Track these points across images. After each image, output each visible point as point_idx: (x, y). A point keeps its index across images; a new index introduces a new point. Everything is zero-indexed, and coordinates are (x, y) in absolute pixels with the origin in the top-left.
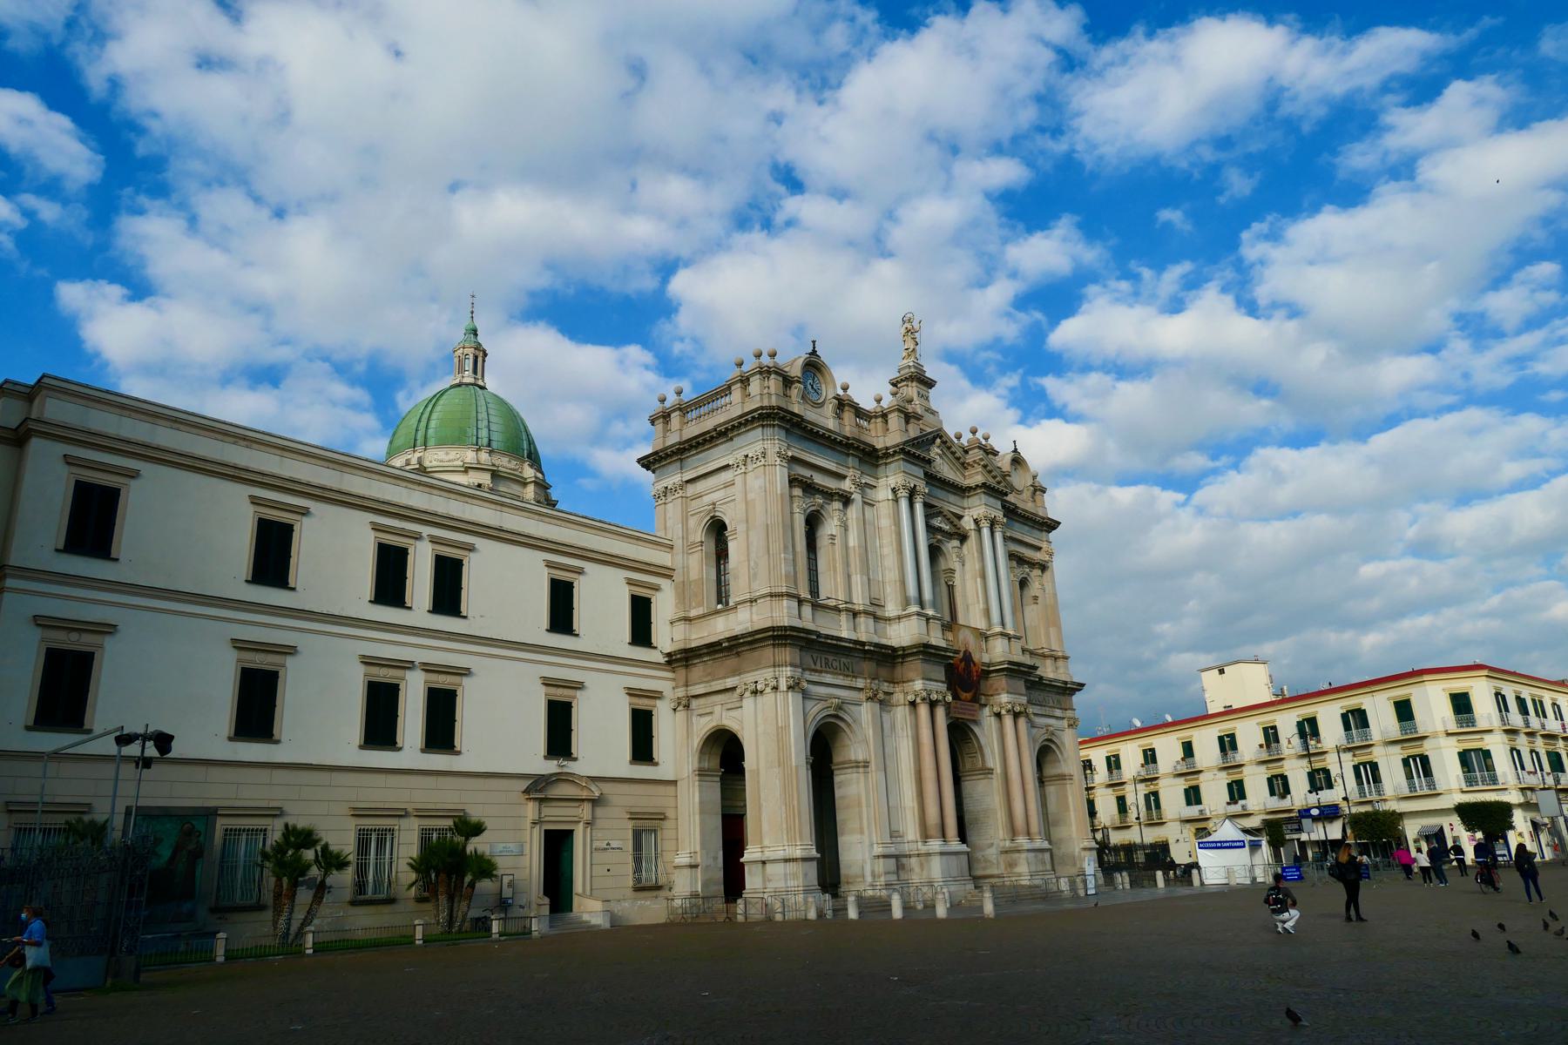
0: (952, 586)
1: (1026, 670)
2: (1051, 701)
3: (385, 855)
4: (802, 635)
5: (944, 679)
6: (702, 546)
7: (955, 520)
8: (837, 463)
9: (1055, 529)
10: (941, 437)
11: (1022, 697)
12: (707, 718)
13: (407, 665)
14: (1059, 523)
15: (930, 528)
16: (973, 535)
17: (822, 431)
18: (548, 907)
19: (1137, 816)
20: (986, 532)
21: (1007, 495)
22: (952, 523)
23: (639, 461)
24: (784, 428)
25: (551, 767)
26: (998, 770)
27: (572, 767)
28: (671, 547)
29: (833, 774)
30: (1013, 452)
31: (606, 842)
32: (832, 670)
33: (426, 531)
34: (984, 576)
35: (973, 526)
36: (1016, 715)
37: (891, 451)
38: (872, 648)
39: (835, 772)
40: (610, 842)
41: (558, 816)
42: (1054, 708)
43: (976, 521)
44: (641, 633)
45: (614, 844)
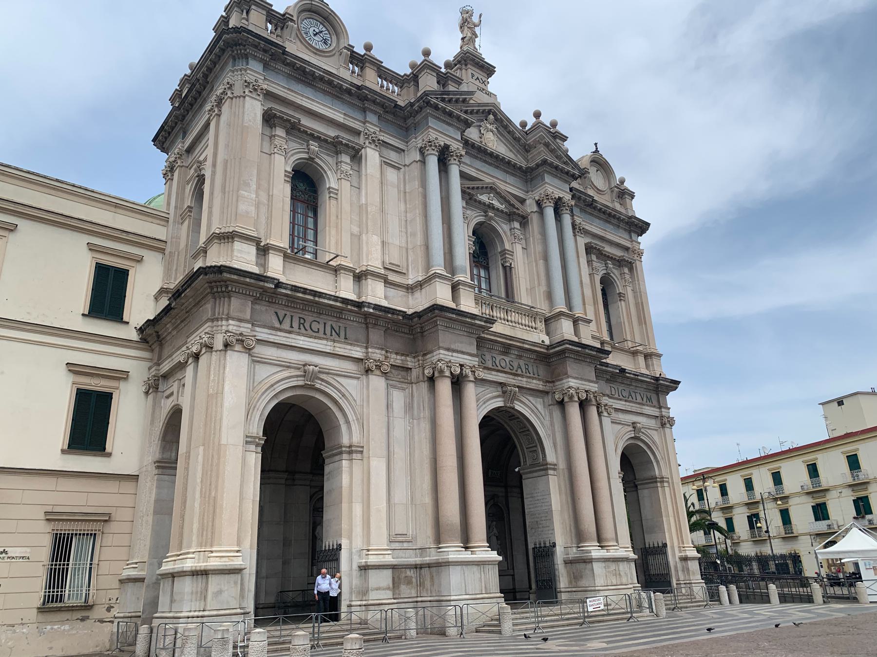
0: (511, 268)
2: (639, 398)
4: (248, 280)
5: (475, 352)
6: (191, 212)
7: (517, 204)
8: (345, 114)
10: (495, 115)
11: (591, 384)
16: (535, 219)
19: (766, 529)
20: (550, 212)
26: (562, 465)
28: (167, 220)
29: (324, 460)
32: (310, 332)
34: (546, 258)
35: (535, 209)
36: (583, 405)
37: (416, 107)
38: (371, 310)
39: (326, 461)
40: (7, 549)
42: (643, 405)
43: (539, 204)
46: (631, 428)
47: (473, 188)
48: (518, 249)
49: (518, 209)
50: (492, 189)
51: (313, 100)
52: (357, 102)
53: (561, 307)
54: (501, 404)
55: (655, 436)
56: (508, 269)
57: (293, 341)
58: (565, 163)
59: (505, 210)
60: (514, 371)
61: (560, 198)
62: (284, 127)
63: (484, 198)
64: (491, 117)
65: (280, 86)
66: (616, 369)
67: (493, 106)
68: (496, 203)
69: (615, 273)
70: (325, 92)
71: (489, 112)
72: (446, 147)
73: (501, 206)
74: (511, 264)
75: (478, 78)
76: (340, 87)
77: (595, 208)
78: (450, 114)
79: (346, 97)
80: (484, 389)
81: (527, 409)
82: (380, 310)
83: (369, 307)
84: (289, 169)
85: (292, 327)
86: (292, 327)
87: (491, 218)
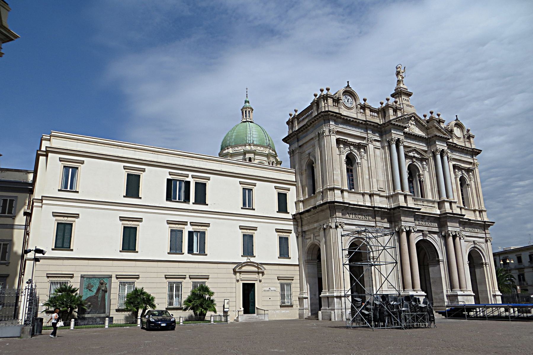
3: (173, 292)
7: (423, 153)
9: (479, 153)
10: (414, 117)
12: (309, 240)
13: (185, 223)
14: (481, 151)
15: (407, 157)
17: (352, 119)
21: (449, 140)
22: (421, 154)
23: (283, 140)
25: (245, 260)
27: (252, 259)
30: (456, 120)
31: (269, 288)
40: (270, 288)
41: (249, 278)
44: (283, 207)
45: (272, 289)
46: (473, 243)
49: (425, 156)
50: (415, 150)
51: (350, 130)
53: (444, 197)
54: (422, 238)
55: (483, 245)
56: (422, 182)
57: (354, 222)
60: (426, 225)
61: (443, 150)
63: (411, 154)
64: (413, 118)
65: (341, 128)
68: (416, 155)
69: (466, 175)
72: (399, 139)
73: (418, 156)
74: (423, 180)
75: (406, 100)
79: (361, 125)
81: (431, 239)
82: (380, 209)
85: (353, 217)
86: (353, 217)
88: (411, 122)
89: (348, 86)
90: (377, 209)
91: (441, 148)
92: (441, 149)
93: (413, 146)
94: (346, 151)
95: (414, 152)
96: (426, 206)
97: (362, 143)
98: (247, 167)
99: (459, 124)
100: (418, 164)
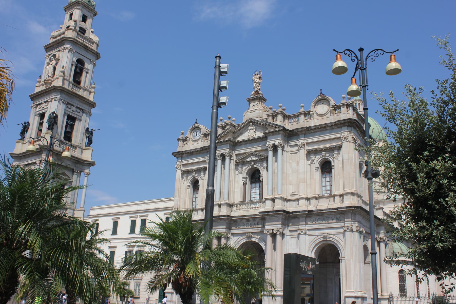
1: (266, 214)
18: (196, 302)
24: (180, 157)
33: (139, 215)
47: (242, 159)
48: (265, 171)
50: (252, 154)
52: (205, 151)
54: (246, 241)
58: (276, 127)
59: (258, 159)
62: (186, 173)
63: (249, 159)
64: (251, 123)
66: (305, 212)
67: (250, 119)
68: (254, 159)
70: (197, 154)
71: (250, 122)
72: (222, 154)
74: (263, 180)
75: (254, 105)
76: (198, 151)
77: (312, 129)
78: (221, 142)
79: (202, 152)
80: (240, 237)
83: (199, 221)
84: (189, 184)
87: (253, 166)
88: (250, 128)
89: (196, 122)
90: (199, 222)
91: (270, 143)
92: (272, 145)
93: (250, 151)
94: (190, 178)
95: (252, 156)
96: (244, 209)
97: (198, 168)
98: (170, 201)
99: (324, 98)
100: (258, 166)
